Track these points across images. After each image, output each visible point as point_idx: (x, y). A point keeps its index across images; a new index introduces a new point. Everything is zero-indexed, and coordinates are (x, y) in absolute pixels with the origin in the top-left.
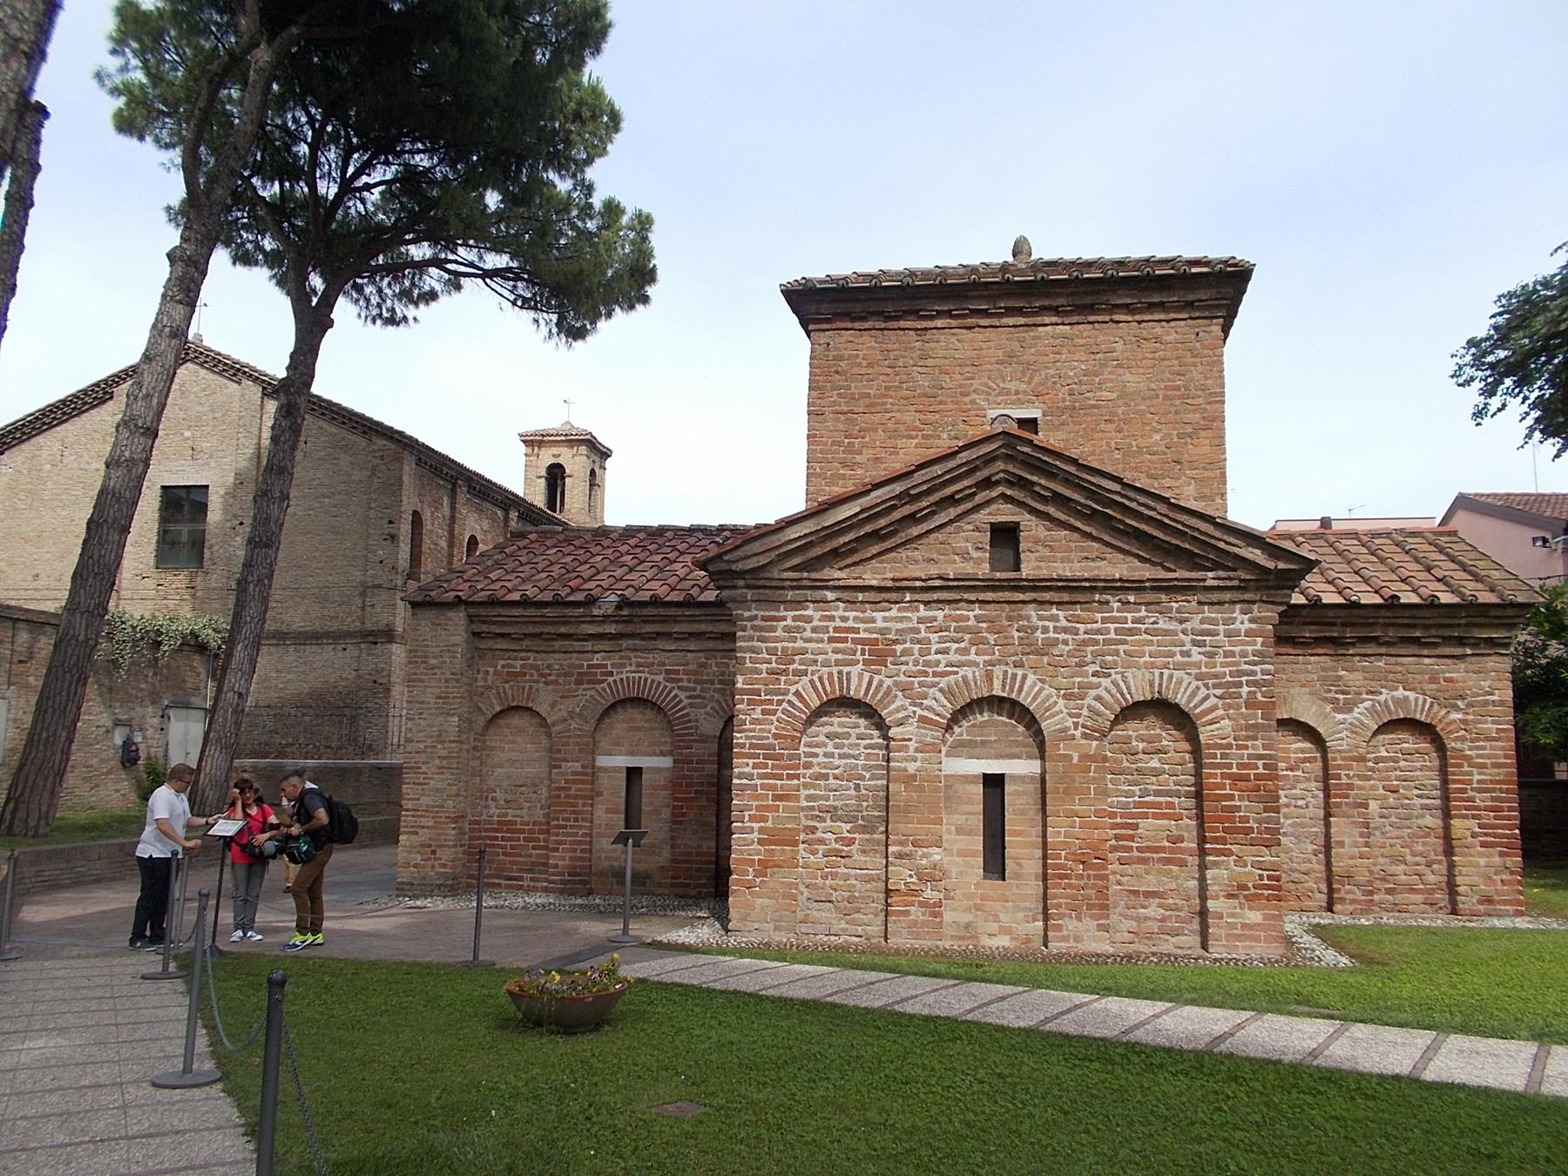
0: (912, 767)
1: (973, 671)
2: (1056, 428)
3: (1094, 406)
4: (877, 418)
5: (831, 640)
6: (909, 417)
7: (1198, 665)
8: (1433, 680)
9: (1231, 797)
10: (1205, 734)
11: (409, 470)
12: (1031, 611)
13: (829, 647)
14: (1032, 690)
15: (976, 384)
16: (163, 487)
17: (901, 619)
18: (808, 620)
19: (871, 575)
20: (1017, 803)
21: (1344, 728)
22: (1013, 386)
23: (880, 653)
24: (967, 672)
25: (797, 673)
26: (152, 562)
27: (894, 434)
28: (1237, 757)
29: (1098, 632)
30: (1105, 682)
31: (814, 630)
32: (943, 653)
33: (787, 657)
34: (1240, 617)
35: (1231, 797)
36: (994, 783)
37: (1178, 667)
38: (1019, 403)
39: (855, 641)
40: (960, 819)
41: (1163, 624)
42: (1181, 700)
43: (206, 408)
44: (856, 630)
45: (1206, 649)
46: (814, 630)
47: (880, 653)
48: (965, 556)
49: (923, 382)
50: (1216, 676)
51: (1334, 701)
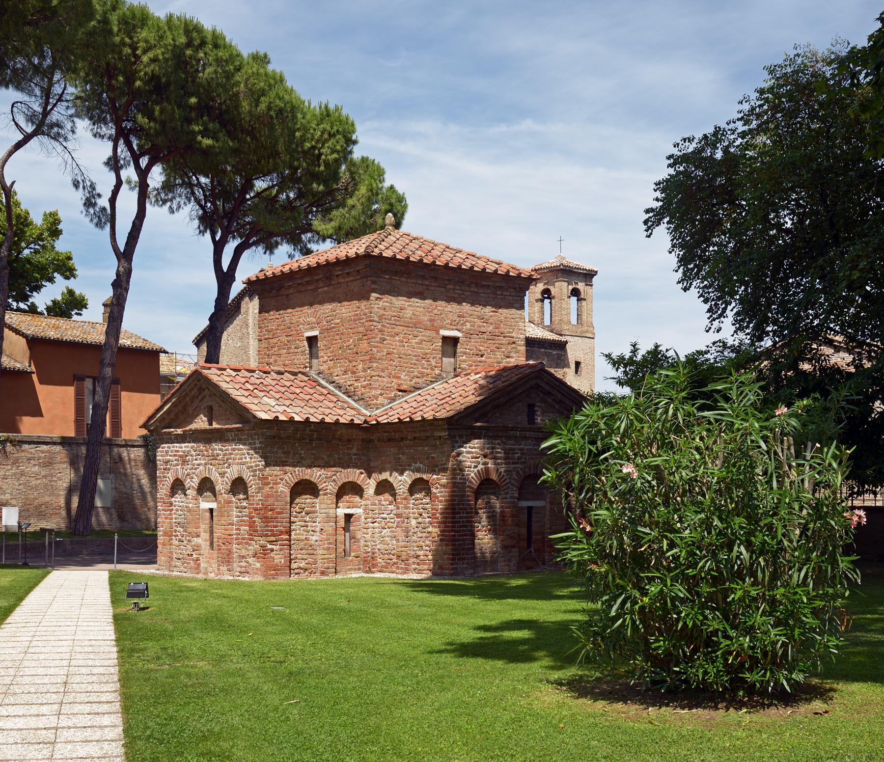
3: (334, 328)
4: (275, 341)
5: (175, 455)
7: (247, 462)
8: (428, 458)
9: (253, 517)
13: (173, 458)
17: (187, 447)
18: (169, 447)
25: (169, 469)
29: (227, 450)
30: (228, 470)
31: (172, 451)
34: (257, 442)
35: (253, 517)
36: (211, 510)
38: (312, 328)
39: (180, 456)
44: (178, 451)
46: (172, 451)
50: (252, 467)
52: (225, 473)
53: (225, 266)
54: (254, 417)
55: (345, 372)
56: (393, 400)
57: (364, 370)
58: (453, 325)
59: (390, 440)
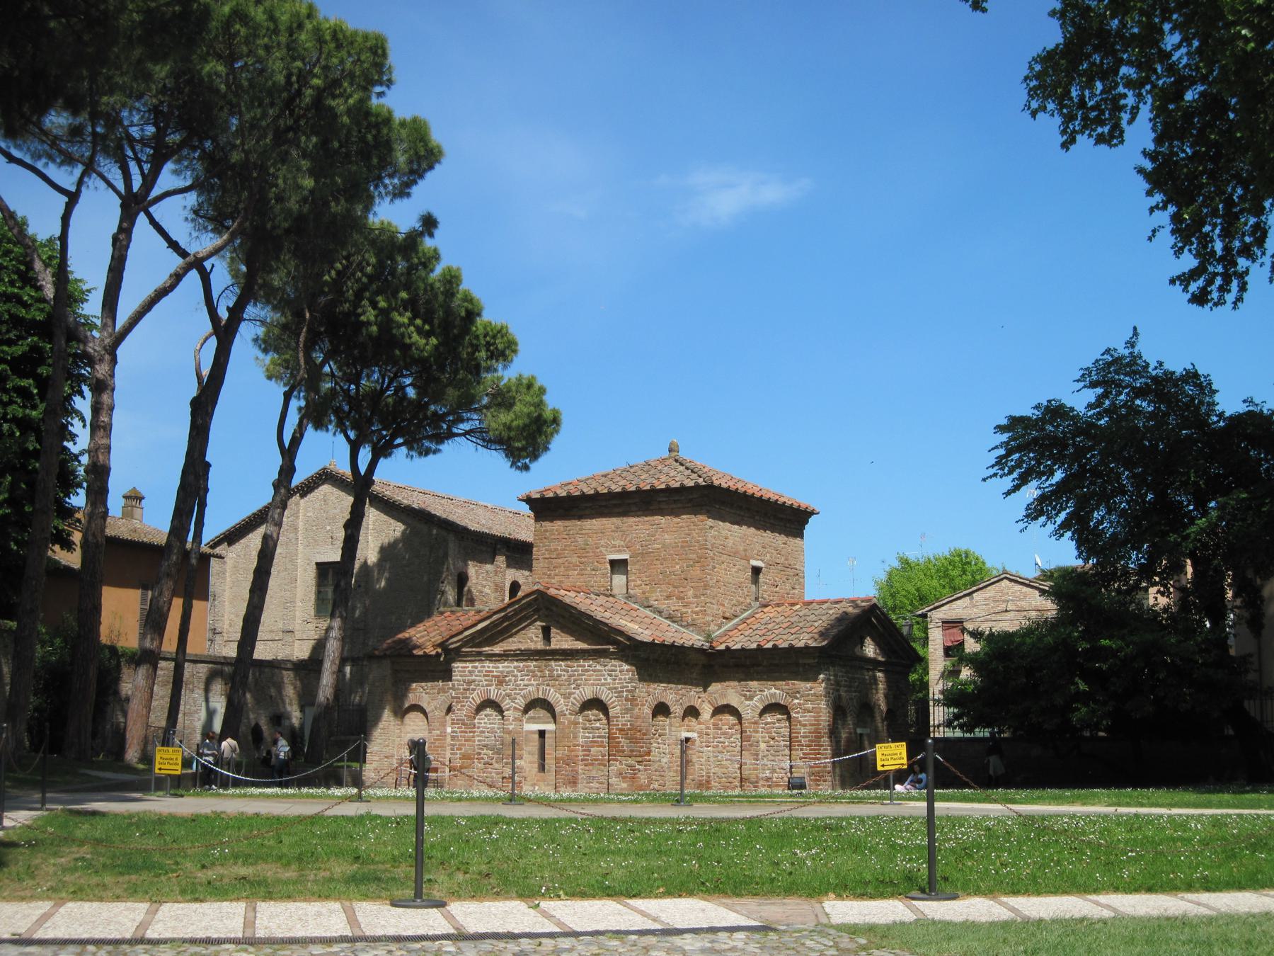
0: (511, 727)
1: (533, 688)
2: (635, 563)
4: (560, 561)
6: (575, 560)
10: (611, 712)
11: (452, 547)
12: (553, 663)
14: (553, 696)
15: (602, 542)
16: (317, 564)
19: (497, 649)
20: (549, 741)
21: (750, 709)
22: (617, 542)
23: (501, 681)
24: (530, 688)
26: (313, 612)
27: (568, 568)
28: (622, 720)
32: (522, 681)
33: (470, 683)
36: (542, 734)
37: (603, 685)
38: (620, 552)
40: (529, 748)
41: (598, 667)
42: (603, 698)
43: (337, 511)
45: (610, 678)
47: (501, 681)
48: (531, 639)
49: (581, 541)
51: (745, 696)
52: (570, 694)
53: (363, 469)
54: (629, 638)
55: (668, 597)
56: (720, 627)
57: (696, 596)
58: (759, 556)
59: (737, 666)
